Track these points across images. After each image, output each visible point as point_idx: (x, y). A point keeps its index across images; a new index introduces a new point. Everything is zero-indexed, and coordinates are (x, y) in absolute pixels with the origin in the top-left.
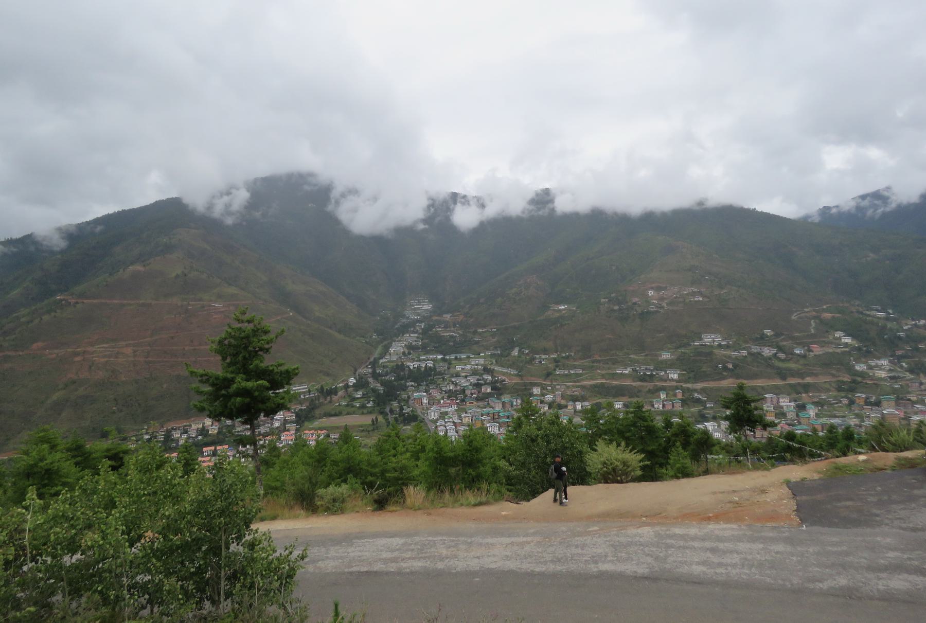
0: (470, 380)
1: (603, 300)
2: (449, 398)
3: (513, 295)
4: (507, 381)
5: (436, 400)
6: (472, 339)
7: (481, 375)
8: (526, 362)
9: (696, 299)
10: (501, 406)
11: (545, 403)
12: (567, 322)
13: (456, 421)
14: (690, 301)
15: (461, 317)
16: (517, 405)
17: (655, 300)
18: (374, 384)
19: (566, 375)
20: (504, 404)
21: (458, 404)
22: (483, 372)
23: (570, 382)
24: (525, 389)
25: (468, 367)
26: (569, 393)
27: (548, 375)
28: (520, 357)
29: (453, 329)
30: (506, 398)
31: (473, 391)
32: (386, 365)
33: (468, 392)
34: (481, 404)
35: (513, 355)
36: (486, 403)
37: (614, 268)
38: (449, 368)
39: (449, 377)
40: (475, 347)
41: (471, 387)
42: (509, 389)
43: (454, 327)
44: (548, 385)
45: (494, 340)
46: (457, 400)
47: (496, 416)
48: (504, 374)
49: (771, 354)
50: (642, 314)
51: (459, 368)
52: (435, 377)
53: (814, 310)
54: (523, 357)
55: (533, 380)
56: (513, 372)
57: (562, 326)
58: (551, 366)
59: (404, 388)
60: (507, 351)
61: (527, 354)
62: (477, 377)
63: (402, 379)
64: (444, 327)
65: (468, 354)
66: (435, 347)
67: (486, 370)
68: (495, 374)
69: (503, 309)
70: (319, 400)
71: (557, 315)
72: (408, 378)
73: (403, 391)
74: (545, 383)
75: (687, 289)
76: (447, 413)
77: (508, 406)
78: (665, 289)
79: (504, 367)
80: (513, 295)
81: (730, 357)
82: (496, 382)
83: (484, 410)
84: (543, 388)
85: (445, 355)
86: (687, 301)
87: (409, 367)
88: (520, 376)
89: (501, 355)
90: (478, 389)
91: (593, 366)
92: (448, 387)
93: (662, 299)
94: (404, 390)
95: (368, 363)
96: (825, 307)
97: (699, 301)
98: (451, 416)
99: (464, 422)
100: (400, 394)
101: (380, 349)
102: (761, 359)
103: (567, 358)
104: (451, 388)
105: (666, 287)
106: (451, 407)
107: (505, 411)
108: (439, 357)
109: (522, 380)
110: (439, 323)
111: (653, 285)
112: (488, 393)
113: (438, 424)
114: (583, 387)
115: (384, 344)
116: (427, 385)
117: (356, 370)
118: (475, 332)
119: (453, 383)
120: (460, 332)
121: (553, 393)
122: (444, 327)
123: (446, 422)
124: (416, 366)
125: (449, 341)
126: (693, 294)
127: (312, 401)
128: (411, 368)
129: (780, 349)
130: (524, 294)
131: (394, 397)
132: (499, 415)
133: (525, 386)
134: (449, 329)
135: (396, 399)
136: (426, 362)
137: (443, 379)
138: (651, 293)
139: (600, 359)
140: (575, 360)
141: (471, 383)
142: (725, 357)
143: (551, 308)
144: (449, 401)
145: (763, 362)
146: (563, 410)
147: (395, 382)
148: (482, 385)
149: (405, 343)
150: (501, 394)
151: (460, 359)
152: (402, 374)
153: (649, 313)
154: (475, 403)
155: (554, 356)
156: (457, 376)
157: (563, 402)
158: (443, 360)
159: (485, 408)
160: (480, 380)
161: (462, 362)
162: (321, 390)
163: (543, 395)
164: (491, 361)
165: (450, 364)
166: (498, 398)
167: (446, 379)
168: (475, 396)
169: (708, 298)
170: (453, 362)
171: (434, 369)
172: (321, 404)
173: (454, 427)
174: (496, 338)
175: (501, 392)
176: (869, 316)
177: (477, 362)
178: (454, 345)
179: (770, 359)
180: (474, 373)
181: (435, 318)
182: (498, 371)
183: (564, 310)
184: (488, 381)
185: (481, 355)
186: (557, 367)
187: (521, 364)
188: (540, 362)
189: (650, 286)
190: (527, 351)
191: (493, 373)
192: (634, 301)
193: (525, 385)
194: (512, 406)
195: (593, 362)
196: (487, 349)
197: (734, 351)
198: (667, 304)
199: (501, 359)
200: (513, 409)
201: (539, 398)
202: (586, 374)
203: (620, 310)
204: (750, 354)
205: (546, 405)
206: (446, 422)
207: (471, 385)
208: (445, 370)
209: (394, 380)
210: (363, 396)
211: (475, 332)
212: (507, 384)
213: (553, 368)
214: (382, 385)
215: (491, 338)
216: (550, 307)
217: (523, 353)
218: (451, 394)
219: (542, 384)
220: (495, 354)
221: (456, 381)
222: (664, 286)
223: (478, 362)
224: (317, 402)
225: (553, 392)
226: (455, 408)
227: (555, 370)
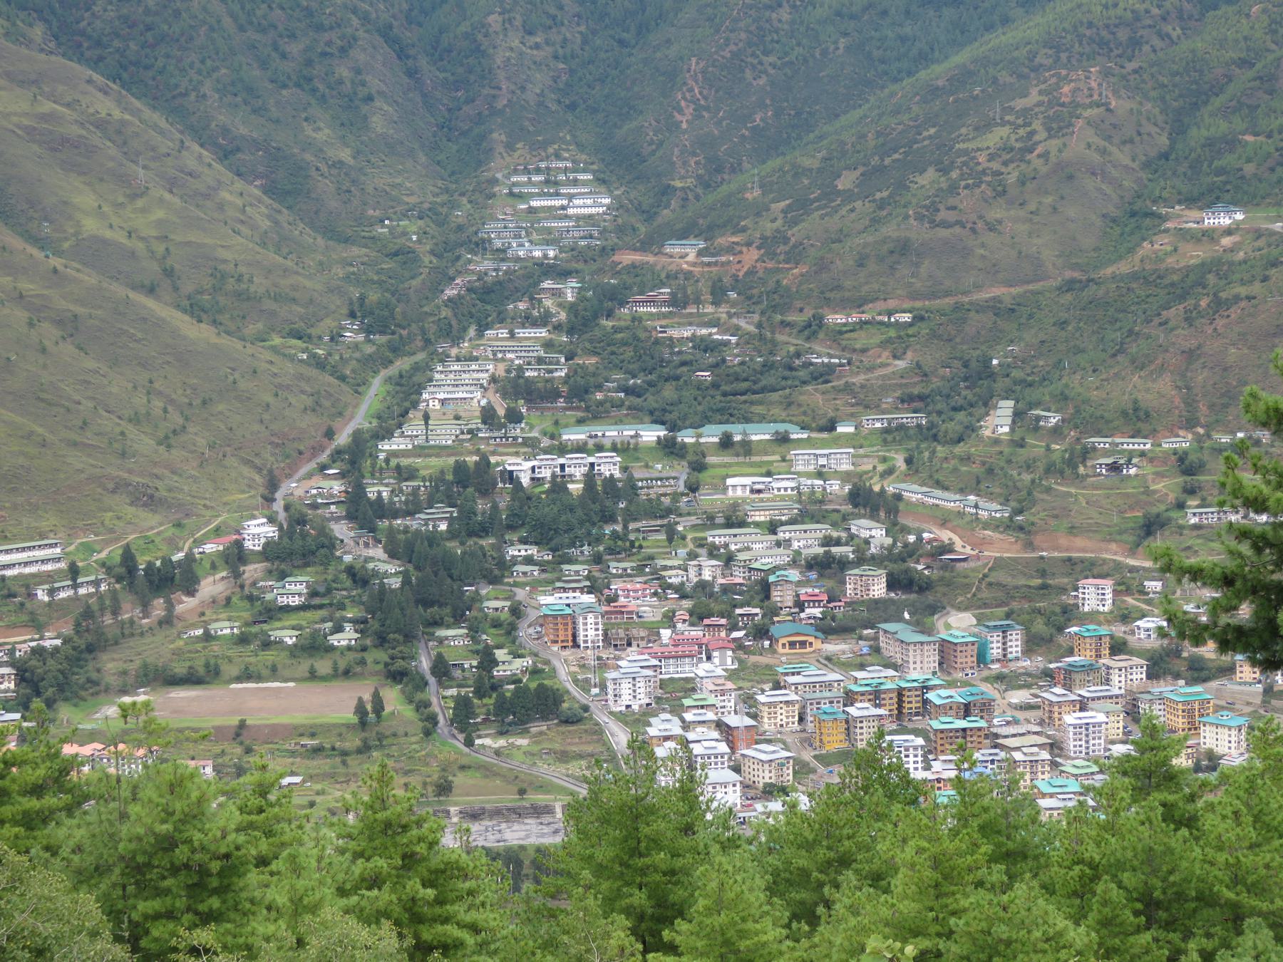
0: (788, 542)
2: (698, 616)
3: (991, 158)
4: (962, 548)
5: (643, 625)
6: (798, 355)
8: (1049, 470)
10: (932, 659)
12: (1243, 291)
13: (733, 720)
15: (751, 256)
16: (1004, 659)
20: (947, 652)
21: (739, 646)
22: (848, 508)
24: (1044, 587)
25: (783, 485)
28: (1021, 444)
29: (710, 309)
32: (408, 467)
33: (784, 597)
35: (987, 433)
36: (864, 647)
38: (693, 488)
39: (695, 527)
40: (813, 396)
41: (794, 575)
42: (968, 586)
43: (716, 303)
44: (1148, 574)
45: (901, 364)
46: (734, 627)
47: (912, 703)
51: (739, 486)
52: (632, 526)
54: (1036, 446)
55: (1082, 548)
56: (991, 509)
57: (1219, 304)
58: (1167, 486)
59: (497, 572)
60: (961, 416)
61: (1056, 432)
62: (823, 530)
63: (483, 531)
64: (674, 301)
65: (782, 427)
66: (628, 391)
68: (903, 520)
69: (945, 225)
70: (115, 612)
71: (1196, 255)
72: (511, 528)
73: (490, 583)
74: (1132, 562)
76: (689, 686)
77: (966, 659)
79: (946, 488)
80: (991, 158)
82: (911, 552)
83: (859, 674)
84: (1127, 585)
85: (673, 428)
87: (510, 477)
88: (1021, 528)
89: (930, 434)
90: (830, 583)
92: (692, 573)
94: (494, 580)
95: (324, 457)
98: (712, 700)
100: (477, 598)
101: (377, 389)
104: (707, 575)
106: (709, 658)
107: (951, 684)
108: (651, 435)
109: (1029, 545)
110: (641, 280)
112: (877, 602)
113: (652, 731)
115: (392, 371)
116: (597, 559)
117: (273, 485)
118: (813, 328)
119: (713, 552)
120: (742, 323)
122: (674, 301)
124: (546, 473)
127: (86, 614)
128: (525, 480)
131: (448, 610)
132: (926, 702)
133: (1043, 573)
134: (692, 309)
135: (458, 619)
137: (672, 535)
141: (798, 552)
143: (1169, 225)
144: (696, 633)
146: (1214, 684)
147: (450, 544)
148: (843, 564)
149: (491, 367)
150: (933, 609)
151: (747, 448)
154: (818, 644)
155: (1182, 442)
156: (729, 524)
158: (669, 448)
159: (862, 667)
160: (838, 543)
161: (755, 459)
163: (1126, 617)
164: (884, 460)
167: (684, 538)
168: (817, 612)
170: (711, 459)
172: (128, 631)
173: (723, 747)
174: (909, 354)
175: (930, 598)
177: (822, 461)
178: (715, 385)
181: (627, 258)
183: (1228, 232)
184: (873, 550)
185: (840, 429)
186: (1191, 491)
187: (1027, 477)
190: (1054, 419)
191: (897, 511)
194: (982, 659)
196: (868, 405)
199: (934, 452)
200: (986, 673)
201: (1104, 631)
205: (1136, 661)
206: (686, 726)
207: (794, 563)
208: (676, 496)
209: (452, 534)
210: (315, 597)
211: (813, 328)
212: (959, 565)
213: (1172, 497)
214: (393, 554)
216: (1163, 218)
219: (1118, 566)
220: (901, 427)
221: (726, 545)
224: (108, 620)
226: (723, 663)
227: (1181, 506)
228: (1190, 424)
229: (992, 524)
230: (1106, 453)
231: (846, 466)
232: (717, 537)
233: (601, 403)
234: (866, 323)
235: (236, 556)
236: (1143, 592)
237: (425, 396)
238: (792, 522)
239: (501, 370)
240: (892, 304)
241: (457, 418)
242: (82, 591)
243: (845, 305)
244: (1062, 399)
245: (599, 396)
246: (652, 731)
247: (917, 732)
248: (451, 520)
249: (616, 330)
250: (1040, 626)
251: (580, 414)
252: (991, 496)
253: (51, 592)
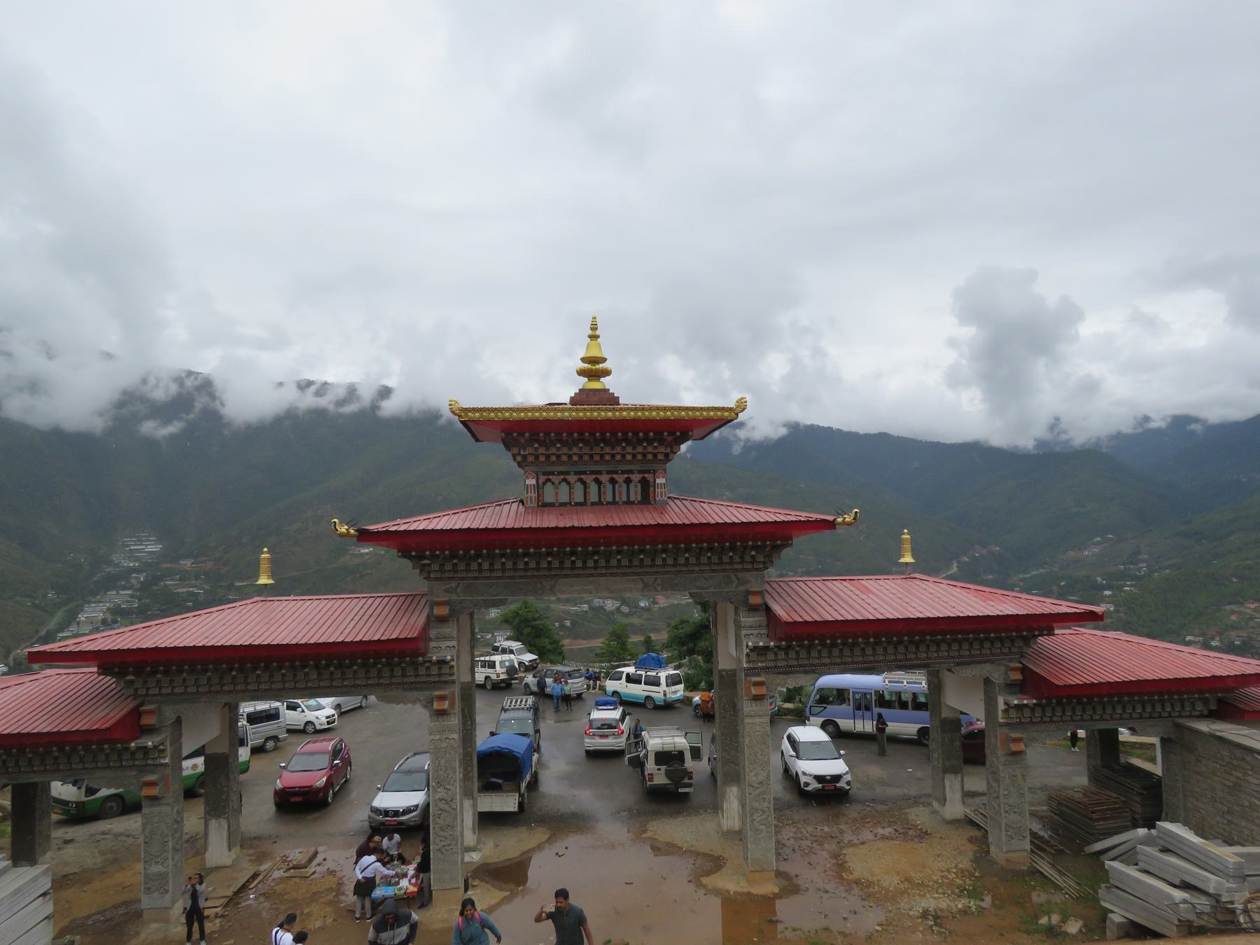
6: (224, 596)
29: (194, 582)
37: (440, 498)
49: (614, 608)
81: (569, 613)
95: (34, 640)
101: (60, 615)
115: (68, 607)
117: (9, 652)
129: (624, 602)
143: (350, 552)
145: (604, 617)
149: (108, 605)
179: (613, 613)
181: (165, 566)
197: (574, 606)
204: (591, 608)
233: (150, 615)
234: (249, 585)
237: (80, 616)
239: (112, 605)
241: (92, 623)
243: (242, 580)
245: (150, 613)
251: (142, 619)
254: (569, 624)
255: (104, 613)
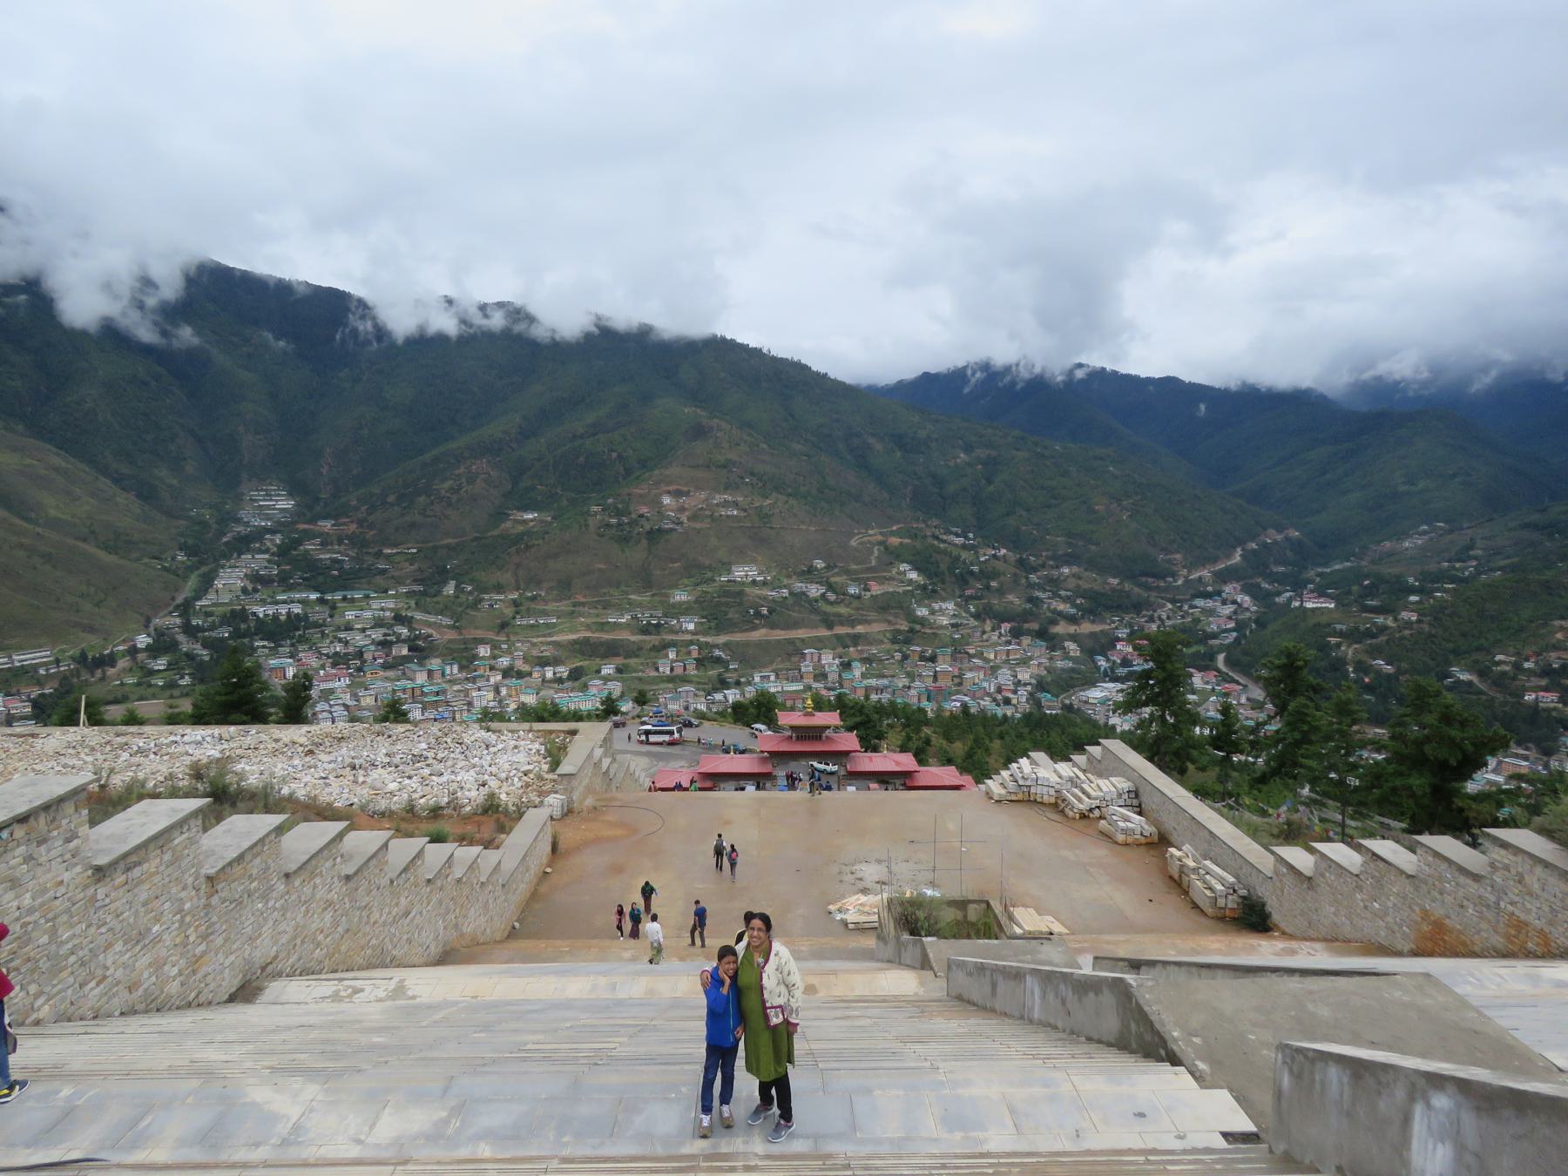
0: (370, 636)
1: (595, 508)
2: (334, 665)
3: (446, 492)
4: (436, 635)
6: (373, 565)
7: (391, 626)
9: (729, 513)
11: (497, 670)
12: (536, 543)
14: (721, 516)
15: (353, 527)
17: (672, 511)
18: (186, 644)
19: (532, 626)
20: (430, 673)
21: (351, 675)
23: (539, 636)
25: (368, 614)
26: (535, 653)
27: (503, 626)
28: (457, 597)
29: (337, 547)
30: (435, 663)
31: (377, 654)
33: (368, 656)
34: (390, 674)
35: (445, 593)
36: (400, 673)
39: (333, 631)
40: (379, 580)
41: (372, 648)
44: (504, 642)
47: (417, 692)
48: (430, 625)
49: (819, 594)
50: (650, 532)
51: (350, 615)
53: (881, 533)
54: (463, 597)
55: (479, 634)
56: (448, 621)
57: (528, 547)
58: (509, 611)
60: (435, 587)
61: (470, 593)
62: (384, 630)
63: (244, 636)
64: (321, 544)
66: (304, 579)
67: (399, 619)
69: (429, 516)
70: (78, 677)
71: (521, 528)
72: (256, 634)
75: (718, 496)
76: (332, 691)
77: (437, 675)
78: (687, 494)
79: (430, 614)
80: (446, 492)
81: (765, 598)
82: (417, 637)
86: (716, 514)
87: (254, 614)
89: (424, 594)
90: (386, 650)
91: (573, 612)
93: (682, 509)
95: (171, 609)
96: (895, 528)
97: (732, 516)
98: (341, 696)
99: (363, 703)
101: (193, 582)
102: (1072, 620)
103: (533, 598)
104: (338, 649)
105: (689, 492)
107: (432, 685)
108: (313, 596)
109: (460, 634)
111: (671, 488)
113: (317, 709)
114: (557, 644)
116: (293, 645)
117: (148, 621)
118: (379, 554)
119: (340, 640)
120: (350, 553)
121: (511, 653)
122: (321, 544)
123: (331, 706)
124: (270, 612)
125: (330, 568)
126: (725, 504)
127: (64, 679)
128: (261, 615)
129: (831, 587)
130: (466, 491)
133: (465, 644)
136: (287, 605)
137: (323, 633)
138: (667, 500)
139: (584, 600)
140: (546, 602)
142: (760, 598)
144: (334, 671)
145: (807, 605)
146: (526, 679)
147: (230, 642)
150: (425, 658)
151: (353, 600)
152: (243, 626)
153: (659, 530)
154: (382, 673)
155: (515, 596)
156: (346, 630)
157: (526, 668)
158: (321, 601)
159: (398, 680)
160: (389, 635)
162: (82, 659)
163: (494, 657)
165: (333, 607)
166: (421, 664)
168: (381, 661)
169: (745, 510)
170: (339, 605)
171: (306, 616)
175: (425, 654)
176: (944, 541)
179: (816, 601)
180: (378, 623)
181: (302, 526)
182: (420, 620)
183: (532, 520)
184: (403, 637)
186: (517, 613)
187: (460, 609)
188: (491, 606)
189: (668, 488)
192: (641, 512)
193: (465, 642)
194: (443, 675)
195: (574, 606)
197: (772, 591)
198: (689, 519)
202: (564, 623)
203: (619, 524)
206: (331, 706)
207: (372, 644)
209: (230, 638)
210: (170, 665)
211: (379, 554)
214: (205, 646)
215: (407, 564)
216: (510, 515)
217: (463, 590)
218: (338, 660)
219: (492, 640)
222: (685, 489)
223: (383, 606)
224: (75, 680)
225: (509, 652)
227: (514, 618)
228: (517, 589)
229: (448, 627)
230: (488, 600)
231: (392, 606)
232: (342, 635)
235: (133, 651)
236: (500, 648)
238: (371, 628)
239: (249, 572)
240: (410, 545)
242: (62, 669)
244: (472, 581)
246: (317, 709)
247: (419, 703)
248: (230, 633)
249: (298, 555)
250: (464, 662)
252: (446, 616)
253: (47, 670)
254: (765, 612)
255: (242, 579)
